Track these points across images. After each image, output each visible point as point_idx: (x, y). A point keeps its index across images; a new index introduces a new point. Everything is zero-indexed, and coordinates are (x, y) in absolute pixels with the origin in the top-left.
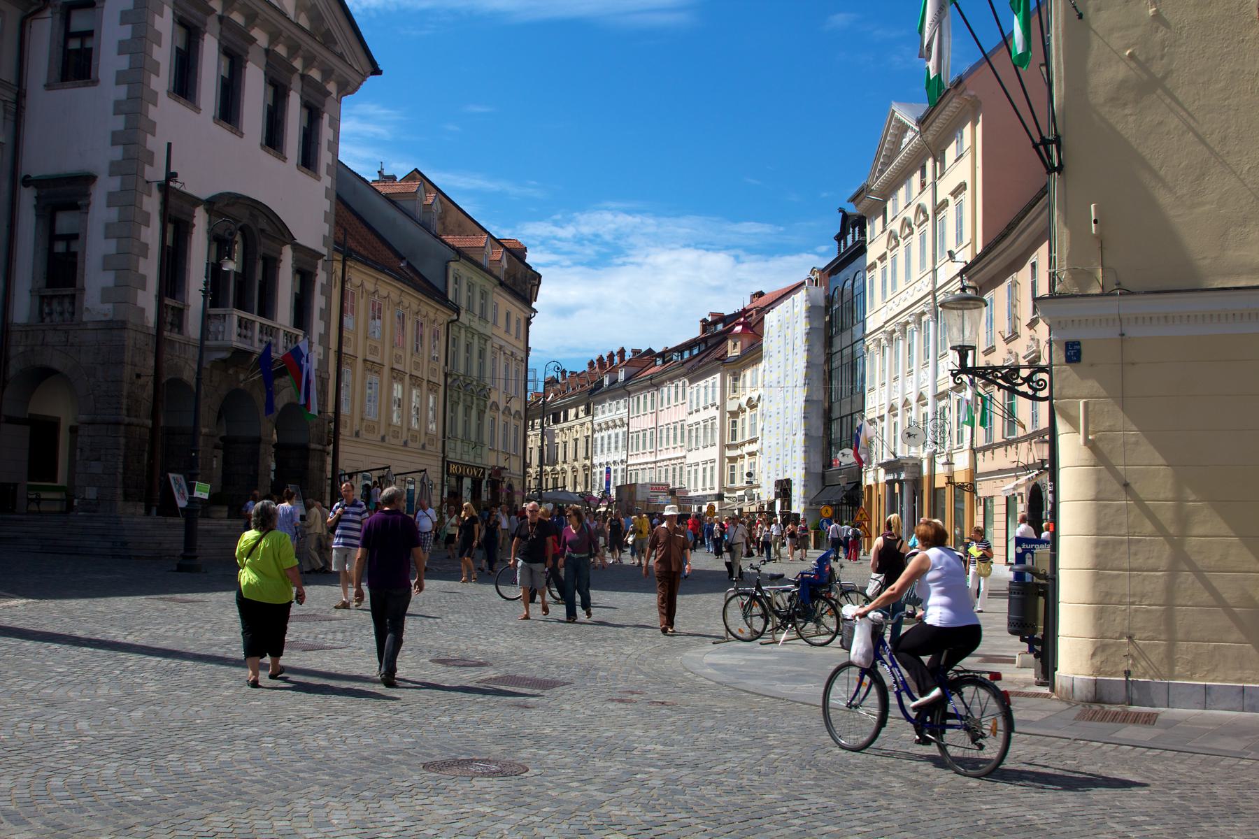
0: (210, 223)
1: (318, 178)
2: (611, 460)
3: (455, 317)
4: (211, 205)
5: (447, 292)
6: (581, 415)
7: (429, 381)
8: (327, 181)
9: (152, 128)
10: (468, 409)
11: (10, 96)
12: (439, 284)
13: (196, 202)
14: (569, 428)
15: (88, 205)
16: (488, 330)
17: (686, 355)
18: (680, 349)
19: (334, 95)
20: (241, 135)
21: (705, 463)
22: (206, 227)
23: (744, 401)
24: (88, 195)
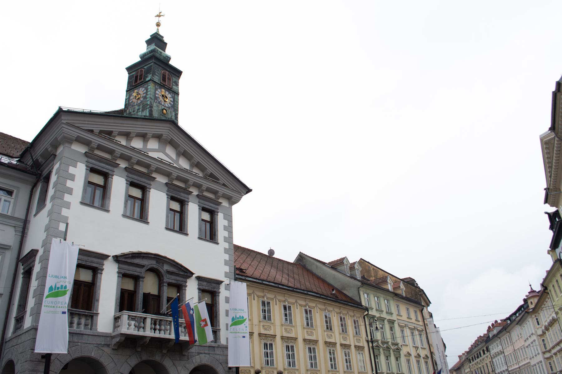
0: (119, 268)
1: (218, 243)
2: (502, 370)
3: (366, 313)
4: (117, 259)
5: (361, 302)
6: (486, 352)
7: (355, 346)
8: (223, 244)
9: (65, 220)
10: (387, 358)
11: (22, 224)
12: (357, 299)
13: (105, 257)
14: (483, 359)
15: (34, 266)
16: (394, 317)
17: (517, 315)
18: (515, 314)
19: (225, 203)
20: (147, 223)
21: (538, 363)
22: (117, 270)
23: (543, 328)
24: (34, 261)
